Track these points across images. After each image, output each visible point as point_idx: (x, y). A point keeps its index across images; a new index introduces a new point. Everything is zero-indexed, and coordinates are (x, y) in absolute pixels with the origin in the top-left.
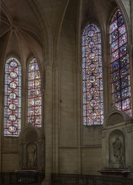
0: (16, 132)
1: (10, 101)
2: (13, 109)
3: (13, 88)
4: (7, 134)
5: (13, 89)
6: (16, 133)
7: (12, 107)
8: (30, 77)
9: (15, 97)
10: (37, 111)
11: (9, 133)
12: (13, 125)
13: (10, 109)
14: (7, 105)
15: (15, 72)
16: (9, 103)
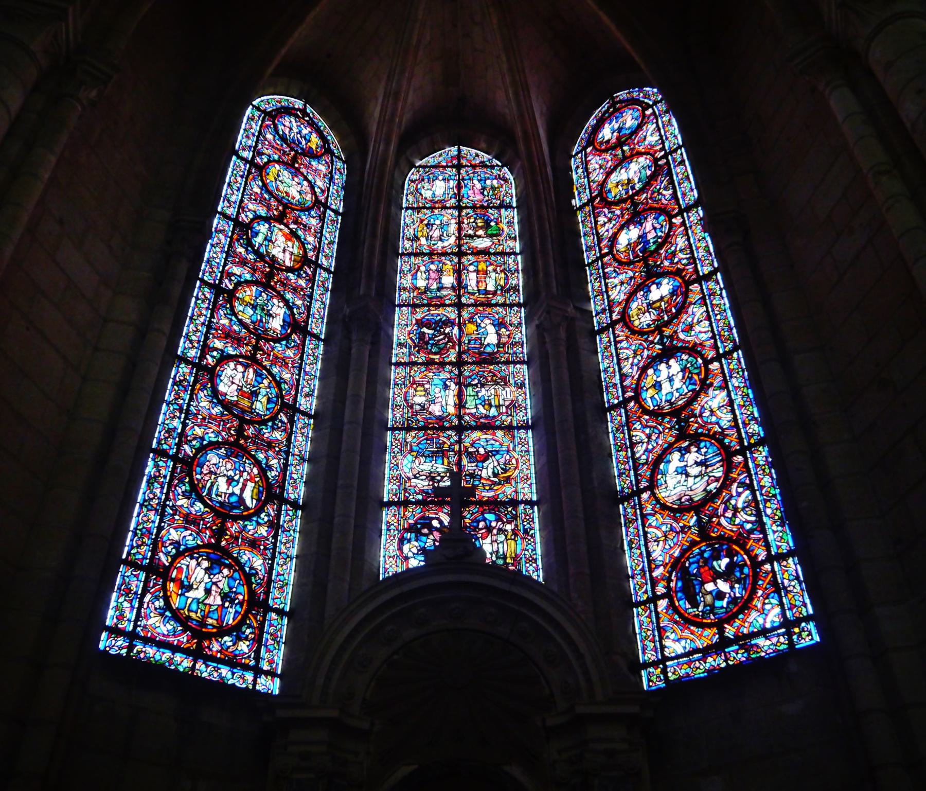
0: (236, 631)
1: (228, 335)
2: (245, 403)
3: (274, 259)
4: (132, 636)
5: (272, 267)
6: (243, 647)
7: (240, 389)
8: (410, 232)
9: (276, 324)
10: (491, 464)
11: (162, 627)
12: (227, 553)
13: (216, 396)
14: (202, 357)
15: (306, 179)
16: (218, 344)
